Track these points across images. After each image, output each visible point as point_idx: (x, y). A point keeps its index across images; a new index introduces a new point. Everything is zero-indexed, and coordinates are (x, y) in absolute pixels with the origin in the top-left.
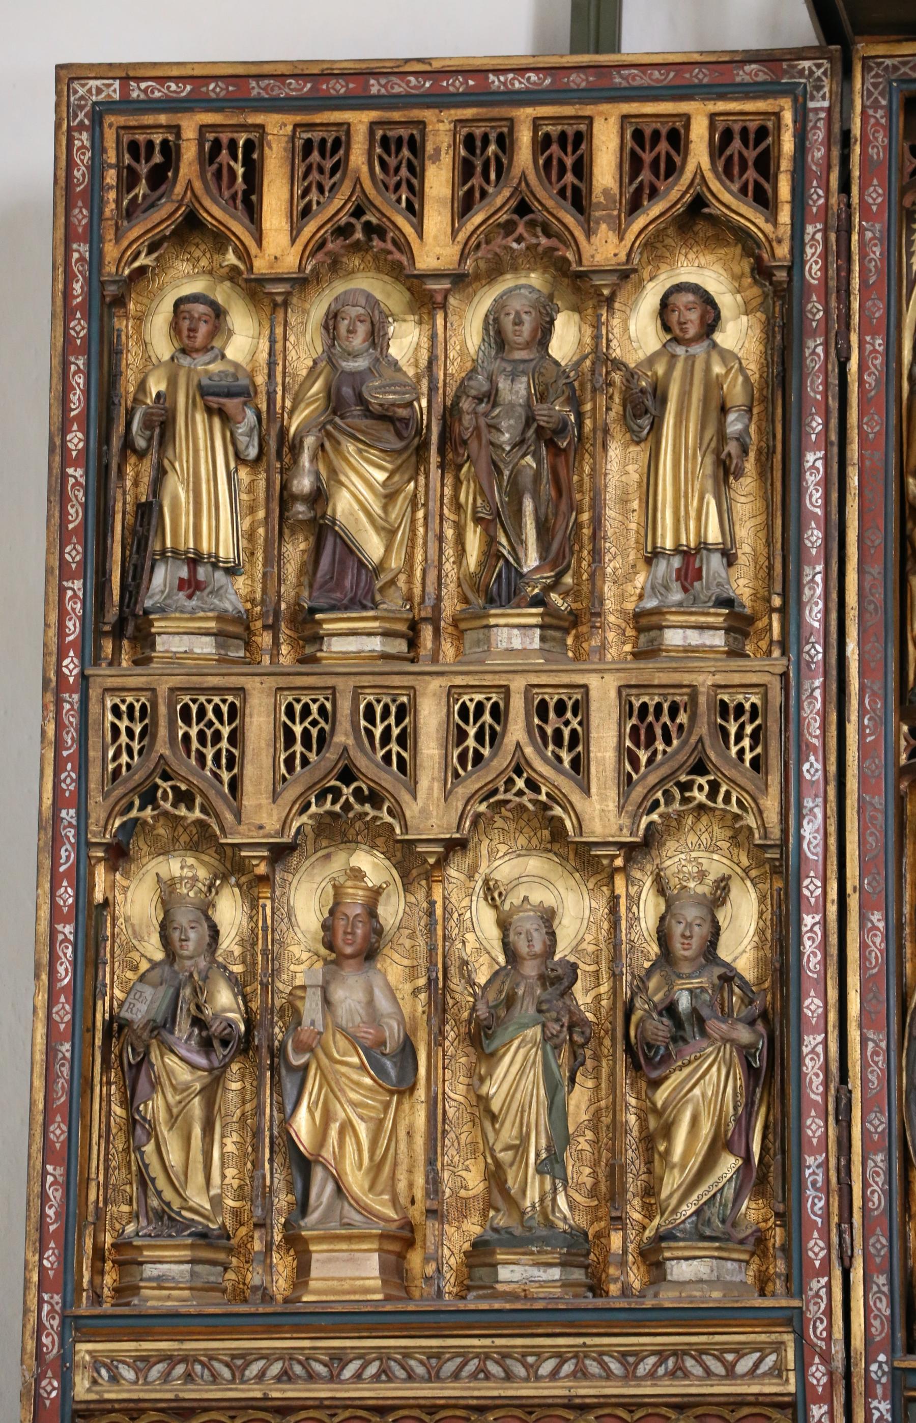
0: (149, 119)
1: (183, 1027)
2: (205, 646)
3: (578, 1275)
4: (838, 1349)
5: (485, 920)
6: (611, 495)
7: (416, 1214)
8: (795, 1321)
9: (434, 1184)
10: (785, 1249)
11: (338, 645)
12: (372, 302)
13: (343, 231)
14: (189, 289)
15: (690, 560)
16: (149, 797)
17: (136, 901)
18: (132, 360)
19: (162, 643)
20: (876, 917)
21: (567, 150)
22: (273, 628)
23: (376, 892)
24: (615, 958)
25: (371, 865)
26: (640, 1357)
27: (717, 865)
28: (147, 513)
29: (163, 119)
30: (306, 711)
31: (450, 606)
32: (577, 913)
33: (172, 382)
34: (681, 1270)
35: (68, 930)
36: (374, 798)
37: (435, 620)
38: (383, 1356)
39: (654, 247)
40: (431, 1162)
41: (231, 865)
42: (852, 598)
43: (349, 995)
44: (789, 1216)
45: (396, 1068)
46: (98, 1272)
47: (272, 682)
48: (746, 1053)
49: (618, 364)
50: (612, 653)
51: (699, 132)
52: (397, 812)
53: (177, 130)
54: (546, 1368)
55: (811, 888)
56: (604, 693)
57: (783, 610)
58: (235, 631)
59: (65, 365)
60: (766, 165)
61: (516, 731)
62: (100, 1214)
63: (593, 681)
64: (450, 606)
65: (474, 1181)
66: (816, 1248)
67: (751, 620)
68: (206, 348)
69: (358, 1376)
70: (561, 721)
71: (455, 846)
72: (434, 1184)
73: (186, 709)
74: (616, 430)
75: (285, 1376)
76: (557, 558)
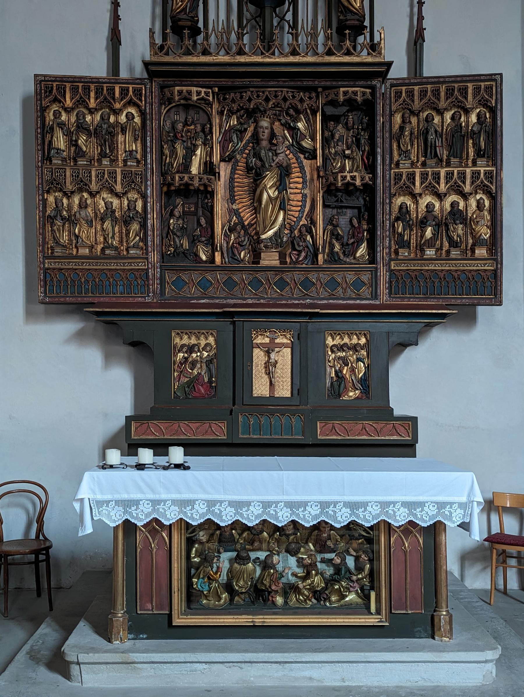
0: (48, 83)
1: (59, 216)
2: (60, 162)
3: (117, 252)
4: (153, 262)
5: (103, 203)
6: (119, 142)
7: (94, 244)
8: (147, 259)
9: (96, 240)
10: (146, 249)
11: (80, 163)
12: (83, 112)
13: (78, 101)
14: (55, 109)
15: (131, 152)
16: (52, 184)
17: (51, 199)
18: (47, 119)
19: (53, 161)
20: (158, 204)
21: (111, 91)
22: (70, 160)
23: (87, 198)
24: (121, 209)
25: (85, 195)
26: (126, 263)
27: (136, 196)
28: (50, 142)
29: (50, 83)
30: (75, 172)
31: (96, 158)
32: (116, 202)
33: (53, 122)
34: (131, 252)
35: (41, 202)
36: (86, 185)
37: (94, 159)
38: (89, 262)
39: (125, 106)
40: (95, 236)
41: (65, 194)
42: (154, 159)
43: (83, 213)
44: (146, 245)
45: (90, 223)
46: (48, 250)
47: (70, 167)
48: (140, 222)
49: (120, 123)
50: (120, 165)
51: (131, 89)
52: (89, 187)
53: (53, 85)
54: (113, 264)
55: (149, 200)
56: (119, 171)
57: (144, 160)
58: (64, 160)
59: (37, 119)
60: (141, 95)
61: (106, 176)
62: (48, 243)
63: (117, 169)
64: (96, 158)
65: (102, 239)
66: (150, 249)
67: (140, 161)
68: (58, 118)
69: (86, 265)
70: (113, 175)
71: (98, 192)
72: (96, 240)
73: (57, 171)
74: (120, 133)
75: (75, 265)
76: (111, 151)
